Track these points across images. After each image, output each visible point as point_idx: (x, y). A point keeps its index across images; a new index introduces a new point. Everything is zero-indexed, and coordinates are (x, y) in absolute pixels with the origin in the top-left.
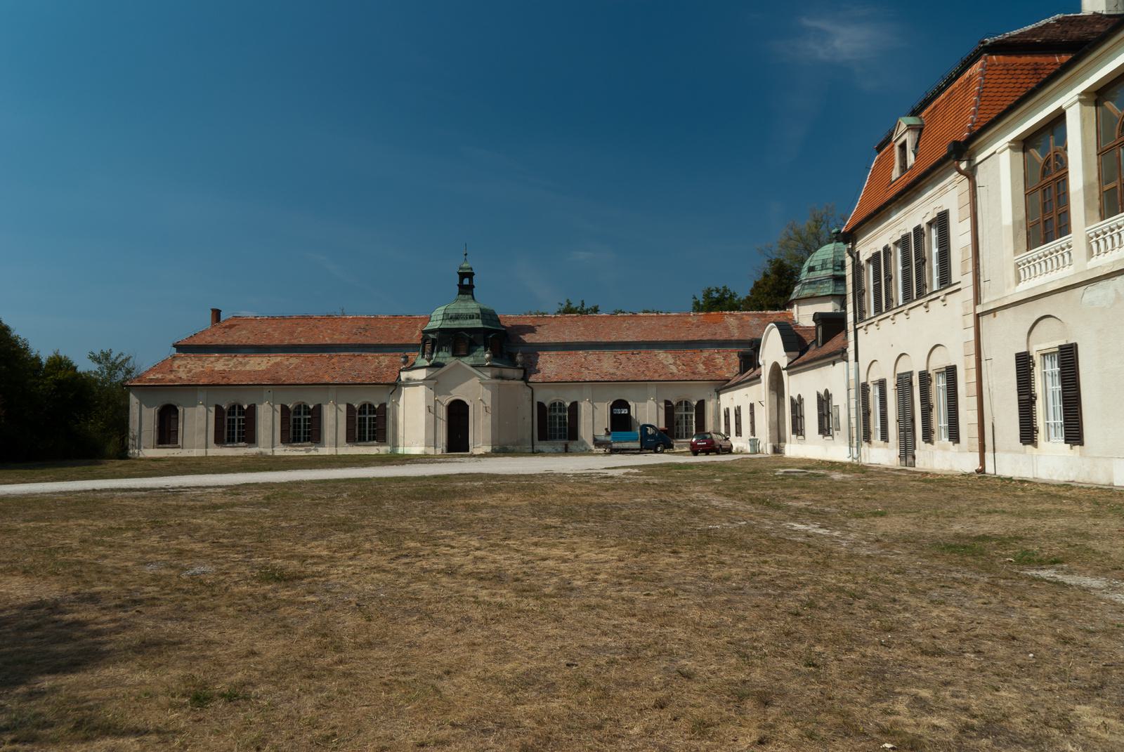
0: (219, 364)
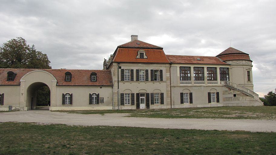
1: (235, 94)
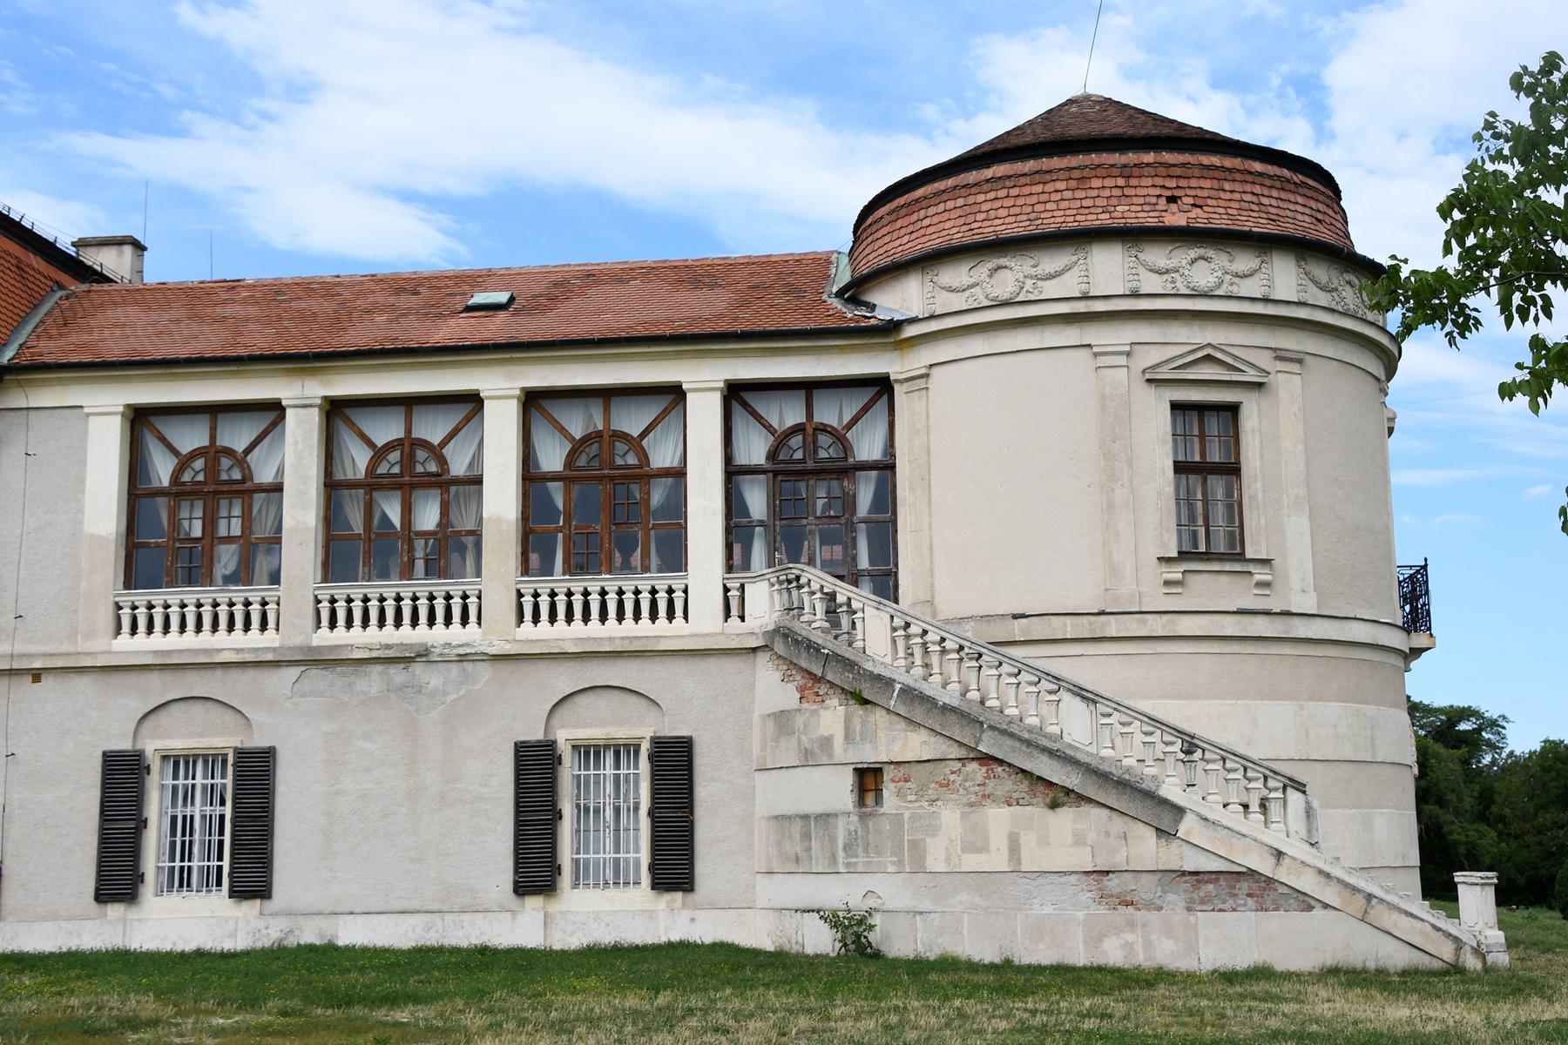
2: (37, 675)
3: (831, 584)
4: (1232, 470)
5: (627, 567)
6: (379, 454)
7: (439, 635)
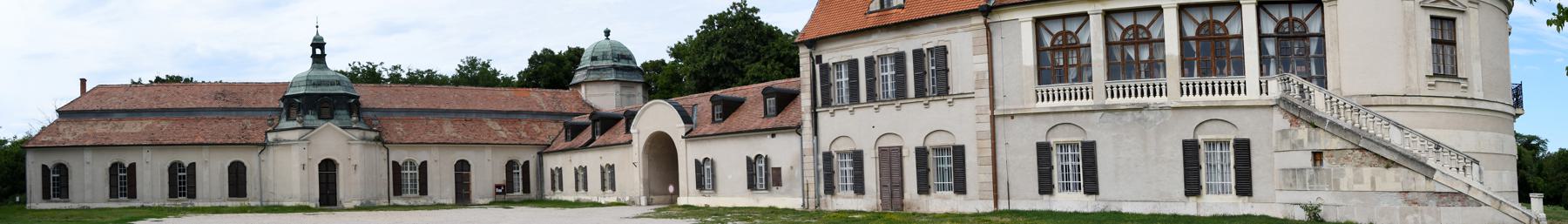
0: (100, 128)
1: (1318, 147)
2: (1012, 117)
3: (1301, 81)
4: (1453, 43)
5: (1222, 74)
6: (1125, 31)
7: (1151, 100)
